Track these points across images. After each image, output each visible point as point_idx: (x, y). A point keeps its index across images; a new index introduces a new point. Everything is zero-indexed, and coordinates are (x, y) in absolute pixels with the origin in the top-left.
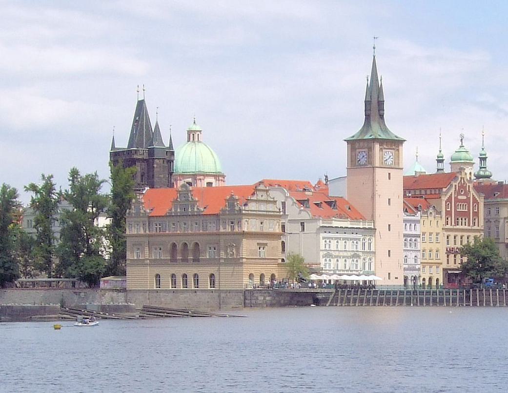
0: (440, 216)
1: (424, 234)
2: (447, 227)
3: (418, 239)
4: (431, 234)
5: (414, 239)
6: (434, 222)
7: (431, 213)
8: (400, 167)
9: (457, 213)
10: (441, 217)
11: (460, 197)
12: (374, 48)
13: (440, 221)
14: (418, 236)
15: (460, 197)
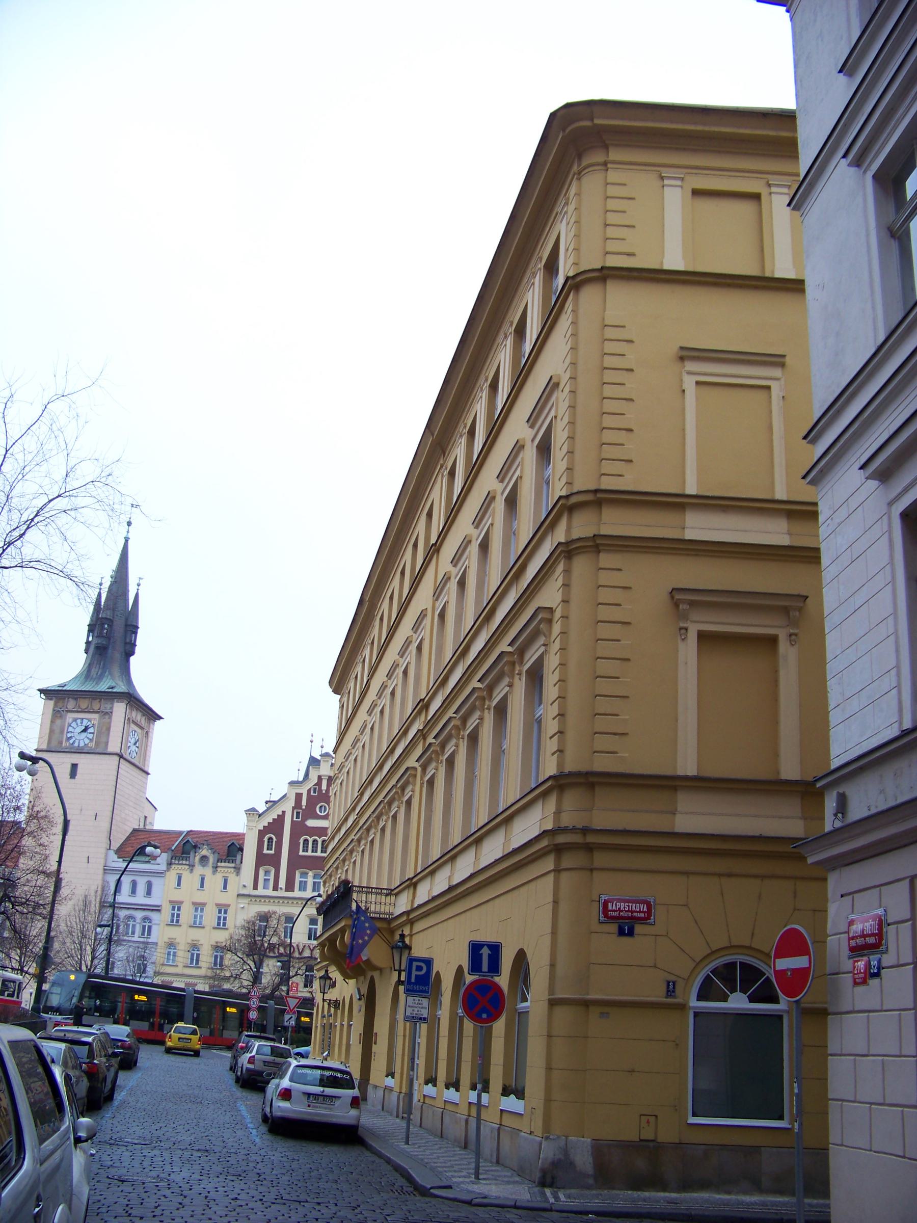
0: (233, 865)
1: (176, 906)
2: (261, 891)
3: (154, 916)
4: (199, 906)
5: (139, 915)
6: (214, 881)
7: (204, 859)
8: (110, 750)
9: (296, 862)
10: (238, 870)
11: (311, 823)
12: (129, 524)
13: (232, 878)
14: (157, 909)
15: (311, 823)
